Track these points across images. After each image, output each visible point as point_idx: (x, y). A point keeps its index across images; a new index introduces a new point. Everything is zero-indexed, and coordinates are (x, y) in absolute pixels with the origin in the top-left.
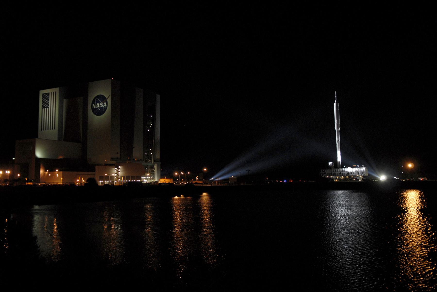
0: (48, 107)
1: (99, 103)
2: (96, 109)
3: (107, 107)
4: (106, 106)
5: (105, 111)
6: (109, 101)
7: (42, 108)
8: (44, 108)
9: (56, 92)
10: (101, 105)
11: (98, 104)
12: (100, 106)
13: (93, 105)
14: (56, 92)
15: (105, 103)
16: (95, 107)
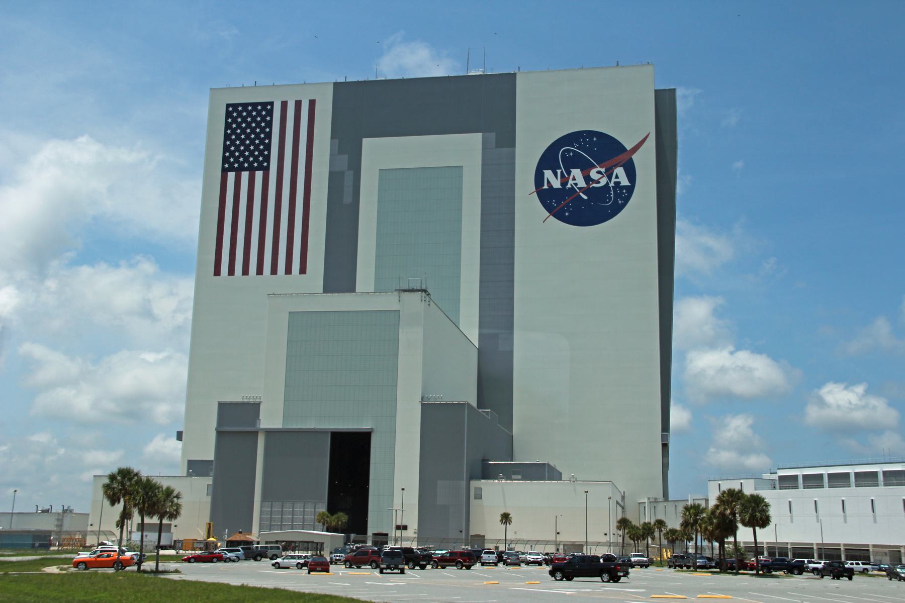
0: (266, 170)
1: (586, 167)
2: (565, 192)
3: (630, 189)
4: (625, 182)
5: (616, 209)
6: (646, 162)
7: (225, 171)
8: (238, 172)
9: (312, 103)
10: (593, 174)
11: (576, 173)
12: (588, 179)
13: (548, 174)
14: (312, 103)
15: (620, 171)
16: (557, 184)
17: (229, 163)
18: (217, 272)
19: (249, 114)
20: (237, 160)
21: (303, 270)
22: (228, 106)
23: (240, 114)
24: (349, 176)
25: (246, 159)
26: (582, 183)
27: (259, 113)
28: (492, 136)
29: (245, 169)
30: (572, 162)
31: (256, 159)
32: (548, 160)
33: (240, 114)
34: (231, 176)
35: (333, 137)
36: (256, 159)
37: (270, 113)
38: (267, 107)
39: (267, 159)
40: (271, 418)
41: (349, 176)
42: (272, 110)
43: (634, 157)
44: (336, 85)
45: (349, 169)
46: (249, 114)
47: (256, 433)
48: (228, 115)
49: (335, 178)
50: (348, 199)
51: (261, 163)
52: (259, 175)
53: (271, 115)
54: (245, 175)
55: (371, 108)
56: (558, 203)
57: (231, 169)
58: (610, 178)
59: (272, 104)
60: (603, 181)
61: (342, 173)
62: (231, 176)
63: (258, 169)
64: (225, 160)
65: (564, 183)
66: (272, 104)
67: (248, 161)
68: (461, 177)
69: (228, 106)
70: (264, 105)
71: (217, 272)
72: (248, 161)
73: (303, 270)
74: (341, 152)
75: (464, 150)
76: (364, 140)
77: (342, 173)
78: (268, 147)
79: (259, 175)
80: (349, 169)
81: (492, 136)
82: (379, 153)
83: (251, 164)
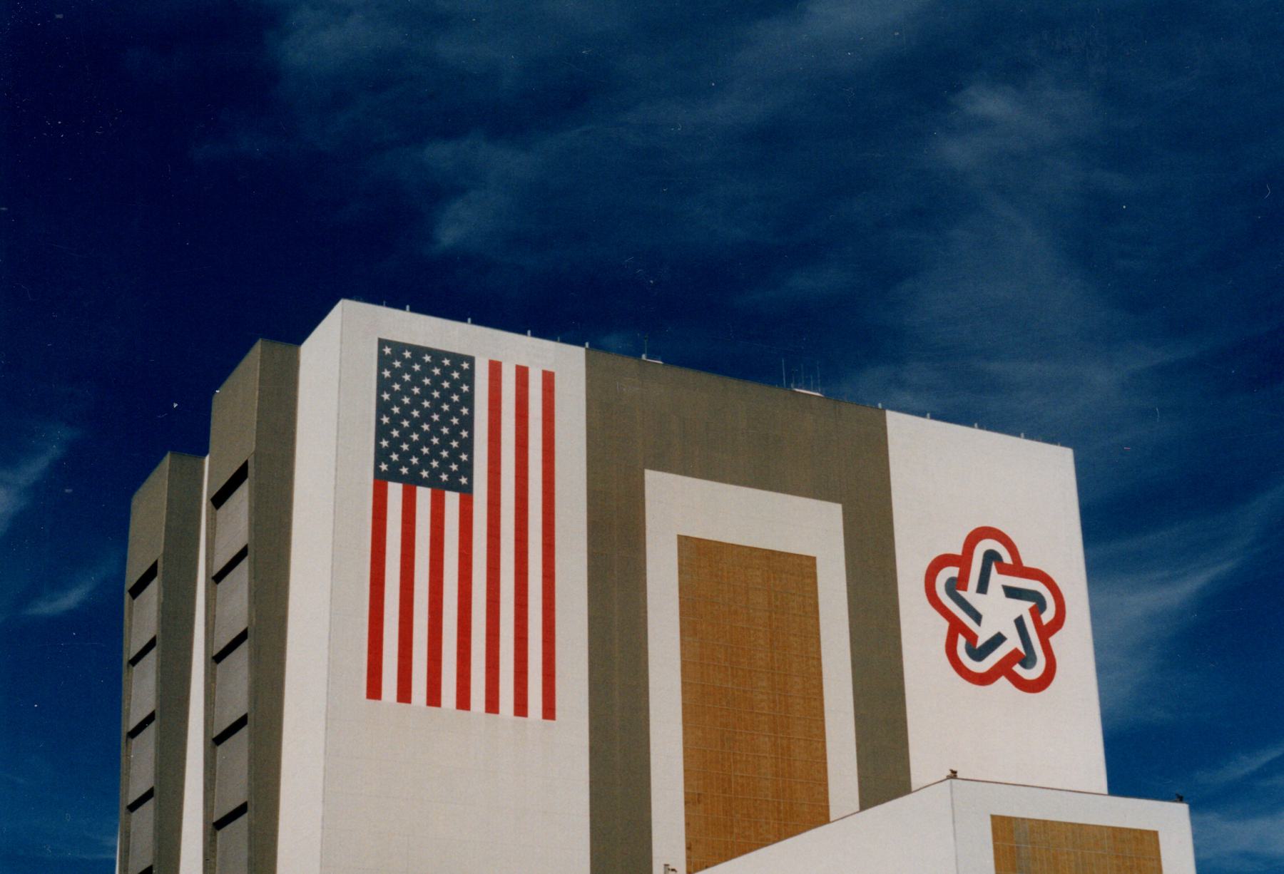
8: (411, 483)
9: (548, 379)
14: (548, 379)
17: (389, 461)
18: (374, 690)
19: (427, 369)
20: (405, 458)
21: (549, 711)
22: (382, 343)
25: (425, 462)
27: (446, 374)
29: (424, 483)
31: (445, 464)
34: (395, 491)
36: (445, 464)
37: (469, 377)
38: (461, 365)
39: (467, 469)
42: (471, 372)
46: (427, 369)
48: (383, 362)
52: (452, 500)
53: (471, 383)
54: (423, 495)
57: (394, 475)
59: (471, 360)
62: (395, 491)
64: (381, 455)
67: (429, 468)
69: (382, 343)
70: (457, 359)
71: (374, 690)
72: (429, 468)
73: (549, 711)
76: (651, 476)
78: (468, 446)
79: (452, 500)
82: (681, 508)
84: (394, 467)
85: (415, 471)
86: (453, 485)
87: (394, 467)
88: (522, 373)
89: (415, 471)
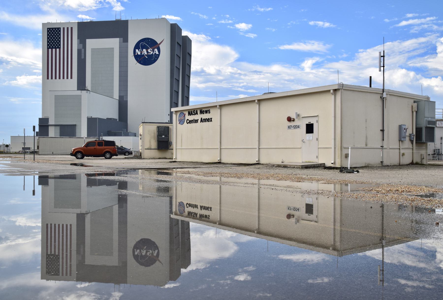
0: (60, 48)
1: (147, 49)
2: (142, 55)
3: (159, 55)
4: (157, 53)
5: (155, 61)
7: (48, 49)
8: (52, 49)
9: (72, 28)
10: (149, 51)
11: (144, 50)
12: (147, 52)
13: (137, 50)
14: (72, 28)
15: (156, 50)
16: (139, 53)
18: (48, 78)
20: (51, 45)
21: (71, 78)
22: (48, 28)
23: (51, 31)
24: (83, 50)
26: (146, 53)
27: (57, 31)
28: (122, 39)
30: (143, 47)
31: (57, 45)
32: (137, 46)
33: (51, 31)
34: (50, 50)
35: (78, 39)
36: (57, 45)
37: (60, 31)
38: (59, 29)
39: (60, 45)
40: (51, 122)
41: (83, 50)
43: (160, 46)
44: (78, 23)
45: (83, 48)
47: (48, 126)
48: (48, 31)
49: (79, 51)
50: (83, 57)
51: (58, 46)
52: (58, 50)
54: (54, 50)
55: (88, 30)
56: (140, 59)
57: (50, 48)
58: (153, 52)
59: (60, 28)
60: (152, 53)
61: (81, 50)
62: (50, 50)
63: (58, 48)
64: (48, 45)
65: (141, 53)
66: (60, 28)
68: (113, 51)
69: (48, 28)
71: (48, 78)
73: (71, 78)
74: (80, 43)
75: (114, 43)
76: (87, 40)
77: (81, 50)
78: (60, 41)
79: (58, 50)
80: (83, 48)
81: (122, 39)
82: (91, 44)
83: (55, 46)
84: (50, 47)
85: (53, 46)
86: (58, 48)
87: (50, 47)
88: (68, 28)
89: (53, 46)
